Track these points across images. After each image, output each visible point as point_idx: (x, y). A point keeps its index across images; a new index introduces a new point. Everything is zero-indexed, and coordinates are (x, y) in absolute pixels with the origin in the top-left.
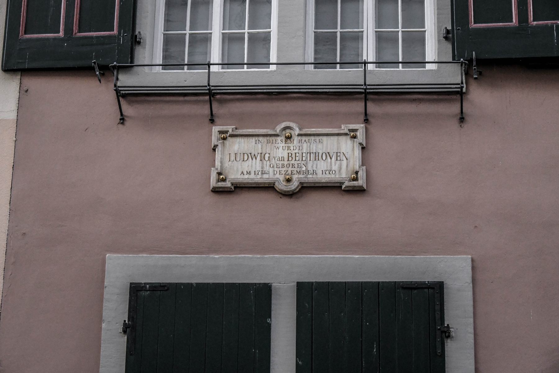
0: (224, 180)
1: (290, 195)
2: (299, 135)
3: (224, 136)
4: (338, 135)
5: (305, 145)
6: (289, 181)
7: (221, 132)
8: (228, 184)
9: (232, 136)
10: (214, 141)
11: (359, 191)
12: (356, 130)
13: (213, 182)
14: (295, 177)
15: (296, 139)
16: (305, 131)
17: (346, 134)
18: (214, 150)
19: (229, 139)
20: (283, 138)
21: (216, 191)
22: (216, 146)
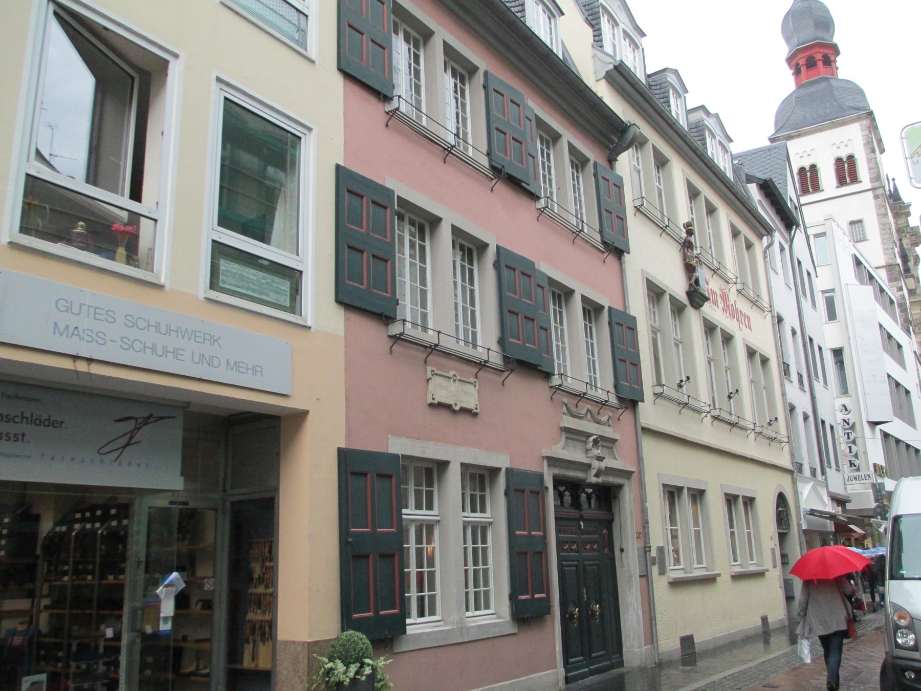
0: (433, 399)
1: (454, 412)
2: (459, 380)
3: (434, 374)
4: (470, 383)
5: (460, 386)
6: (456, 404)
7: (432, 371)
8: (436, 402)
9: (437, 374)
10: (429, 375)
11: (476, 415)
12: (475, 382)
13: (430, 401)
14: (458, 403)
15: (457, 382)
16: (463, 379)
17: (473, 384)
18: (428, 380)
19: (435, 376)
20: (452, 380)
21: (431, 405)
22: (430, 378)
